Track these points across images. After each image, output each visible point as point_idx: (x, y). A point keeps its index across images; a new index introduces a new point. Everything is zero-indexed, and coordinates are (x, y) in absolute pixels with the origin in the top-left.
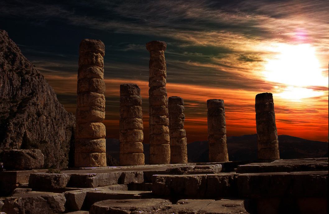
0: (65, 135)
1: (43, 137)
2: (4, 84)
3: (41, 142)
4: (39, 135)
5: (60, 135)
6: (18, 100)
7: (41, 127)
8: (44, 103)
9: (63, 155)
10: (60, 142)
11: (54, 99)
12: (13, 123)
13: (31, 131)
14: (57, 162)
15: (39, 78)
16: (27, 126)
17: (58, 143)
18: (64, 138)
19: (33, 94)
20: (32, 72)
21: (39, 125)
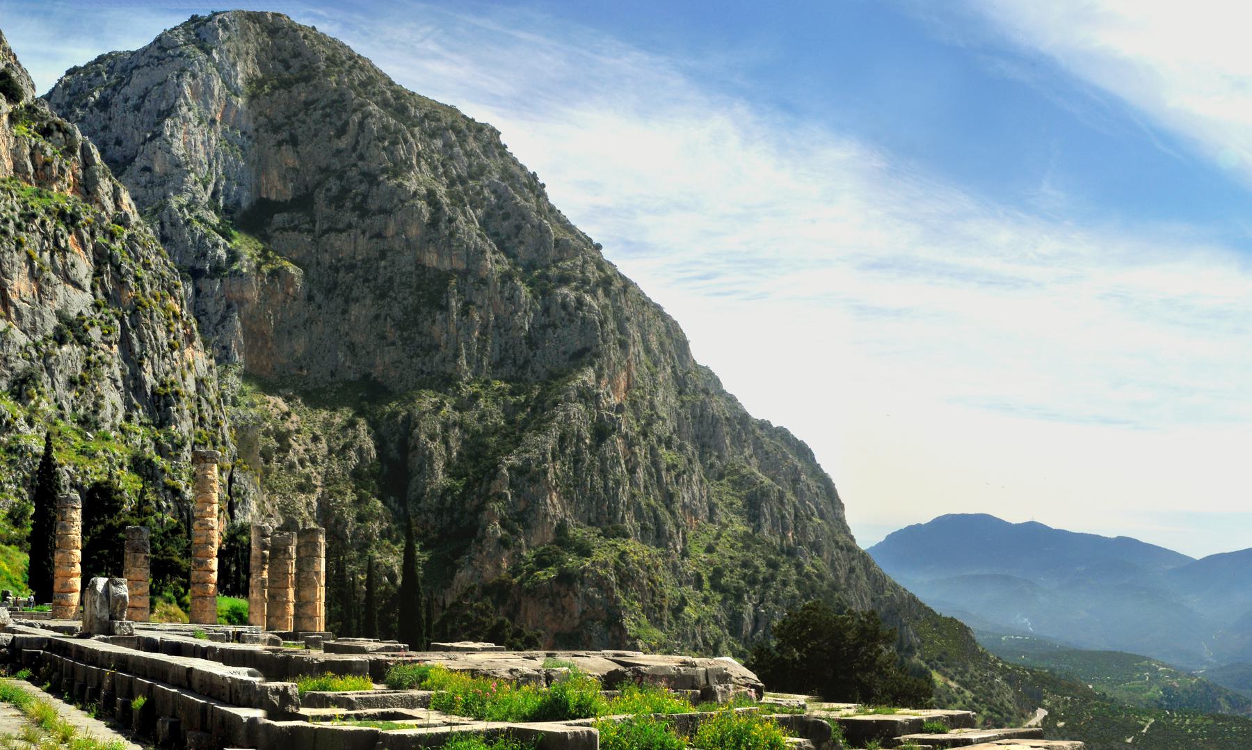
1: (615, 516)
2: (486, 327)
3: (606, 535)
5: (684, 506)
9: (688, 582)
10: (684, 534)
12: (510, 469)
15: (607, 294)
17: (671, 536)
18: (703, 515)
19: (582, 356)
20: (582, 272)
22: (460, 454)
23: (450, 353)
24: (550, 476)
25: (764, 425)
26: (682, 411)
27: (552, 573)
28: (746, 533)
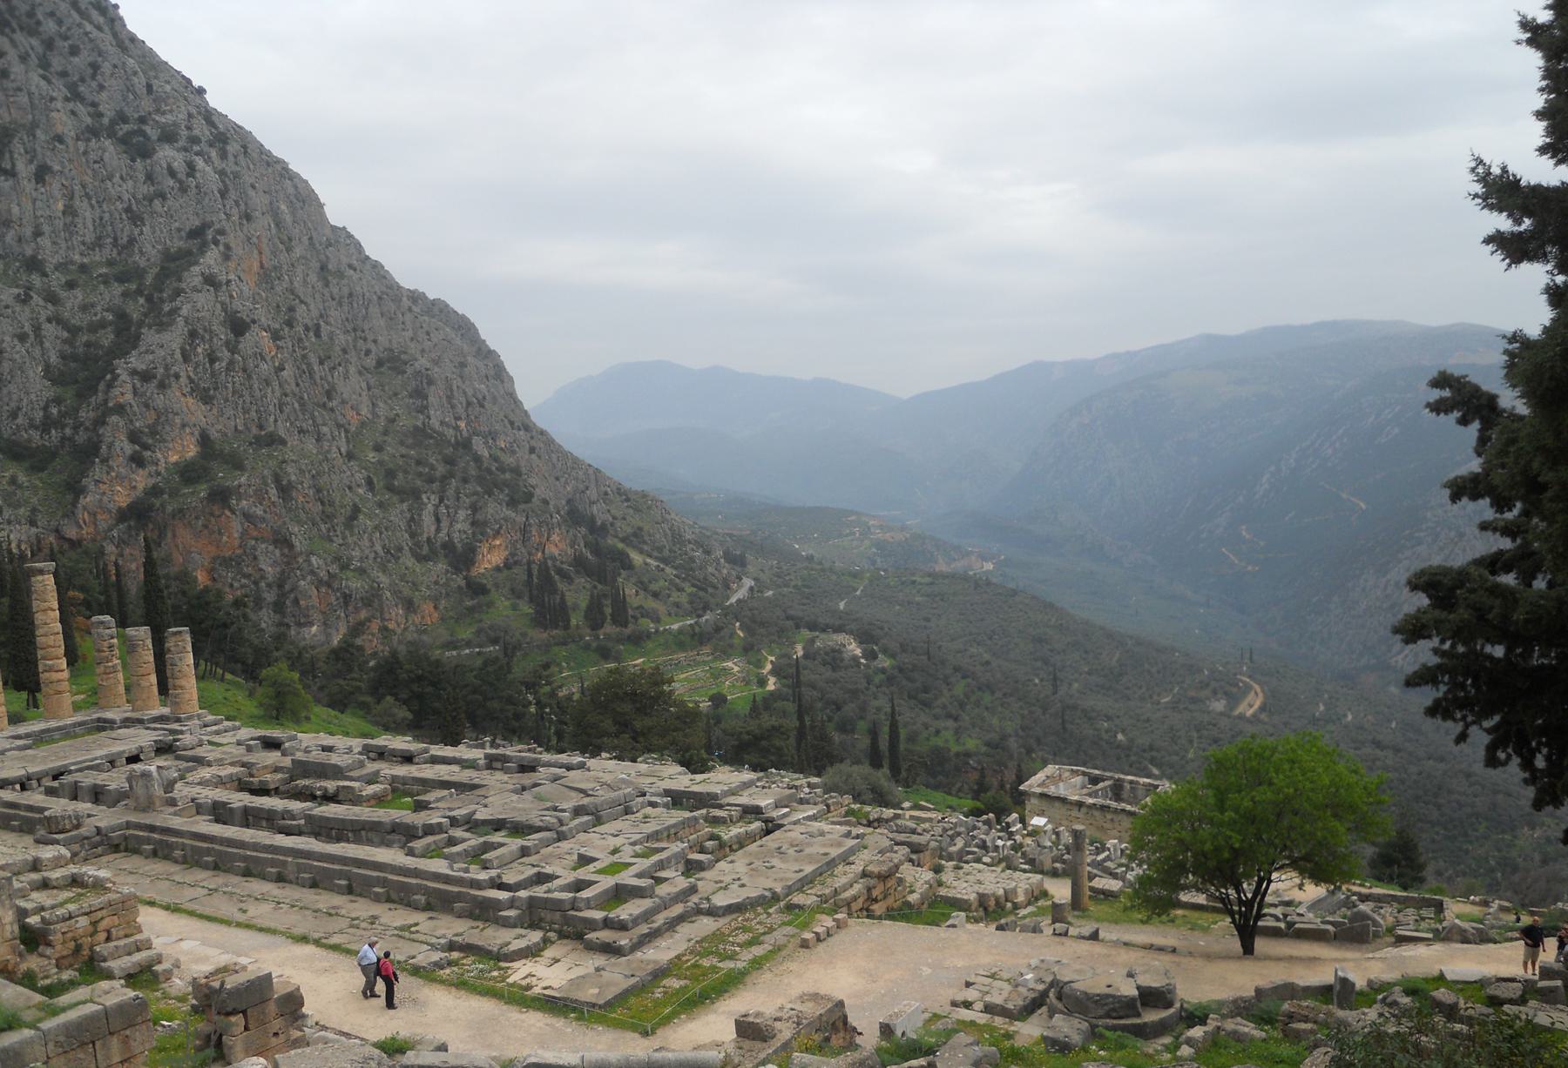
0: (365, 398)
4: (246, 411)
5: (343, 402)
6: (143, 263)
7: (249, 377)
8: (262, 267)
10: (347, 431)
11: (311, 239)
13: (213, 398)
14: (327, 517)
16: (191, 381)
18: (364, 411)
21: (245, 370)
22: (63, 357)
23: (28, 231)
24: (183, 380)
25: (416, 297)
26: (326, 292)
27: (203, 490)
28: (416, 428)
